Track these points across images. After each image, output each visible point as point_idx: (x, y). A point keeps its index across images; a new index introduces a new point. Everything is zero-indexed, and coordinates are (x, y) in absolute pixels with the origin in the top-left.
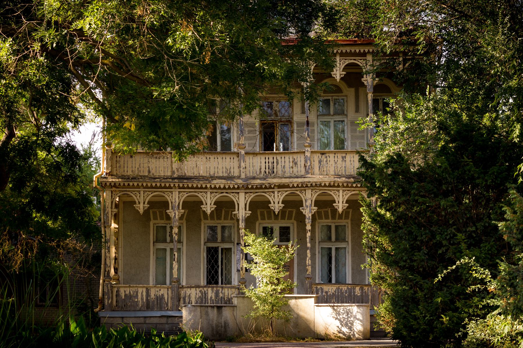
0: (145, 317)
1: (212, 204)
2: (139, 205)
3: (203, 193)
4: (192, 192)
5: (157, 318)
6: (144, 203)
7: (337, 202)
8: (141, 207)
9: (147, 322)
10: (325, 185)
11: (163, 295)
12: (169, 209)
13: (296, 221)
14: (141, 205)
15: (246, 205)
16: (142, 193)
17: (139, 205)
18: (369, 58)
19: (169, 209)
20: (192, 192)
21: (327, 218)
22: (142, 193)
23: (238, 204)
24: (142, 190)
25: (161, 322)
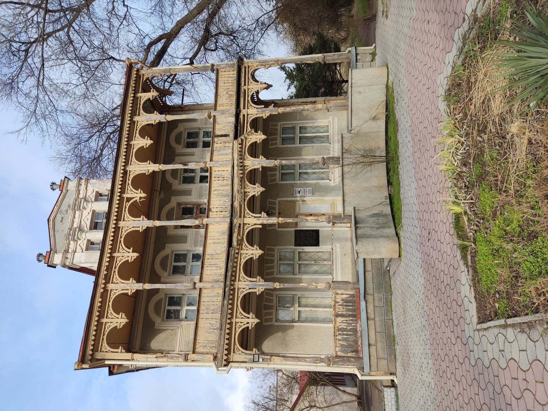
0: (368, 319)
1: (253, 248)
2: (250, 323)
3: (242, 257)
4: (240, 268)
5: (368, 305)
6: (248, 318)
7: (256, 140)
8: (253, 320)
9: (373, 317)
10: (241, 148)
11: (342, 300)
12: (256, 292)
13: (277, 198)
14: (250, 320)
15: (255, 217)
16: (237, 320)
17: (250, 323)
18: (136, 118)
19: (256, 292)
20: (240, 268)
21: (275, 175)
22: (237, 320)
23: (255, 224)
24: (234, 320)
25: (372, 301)
